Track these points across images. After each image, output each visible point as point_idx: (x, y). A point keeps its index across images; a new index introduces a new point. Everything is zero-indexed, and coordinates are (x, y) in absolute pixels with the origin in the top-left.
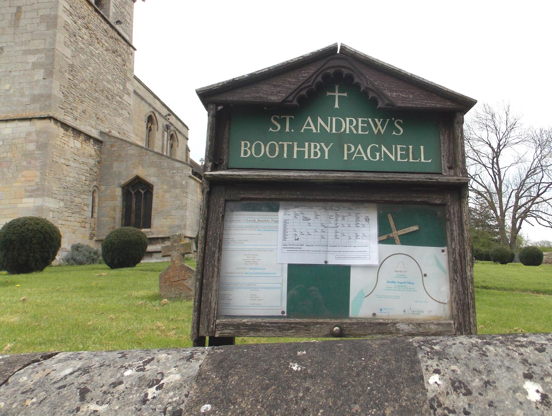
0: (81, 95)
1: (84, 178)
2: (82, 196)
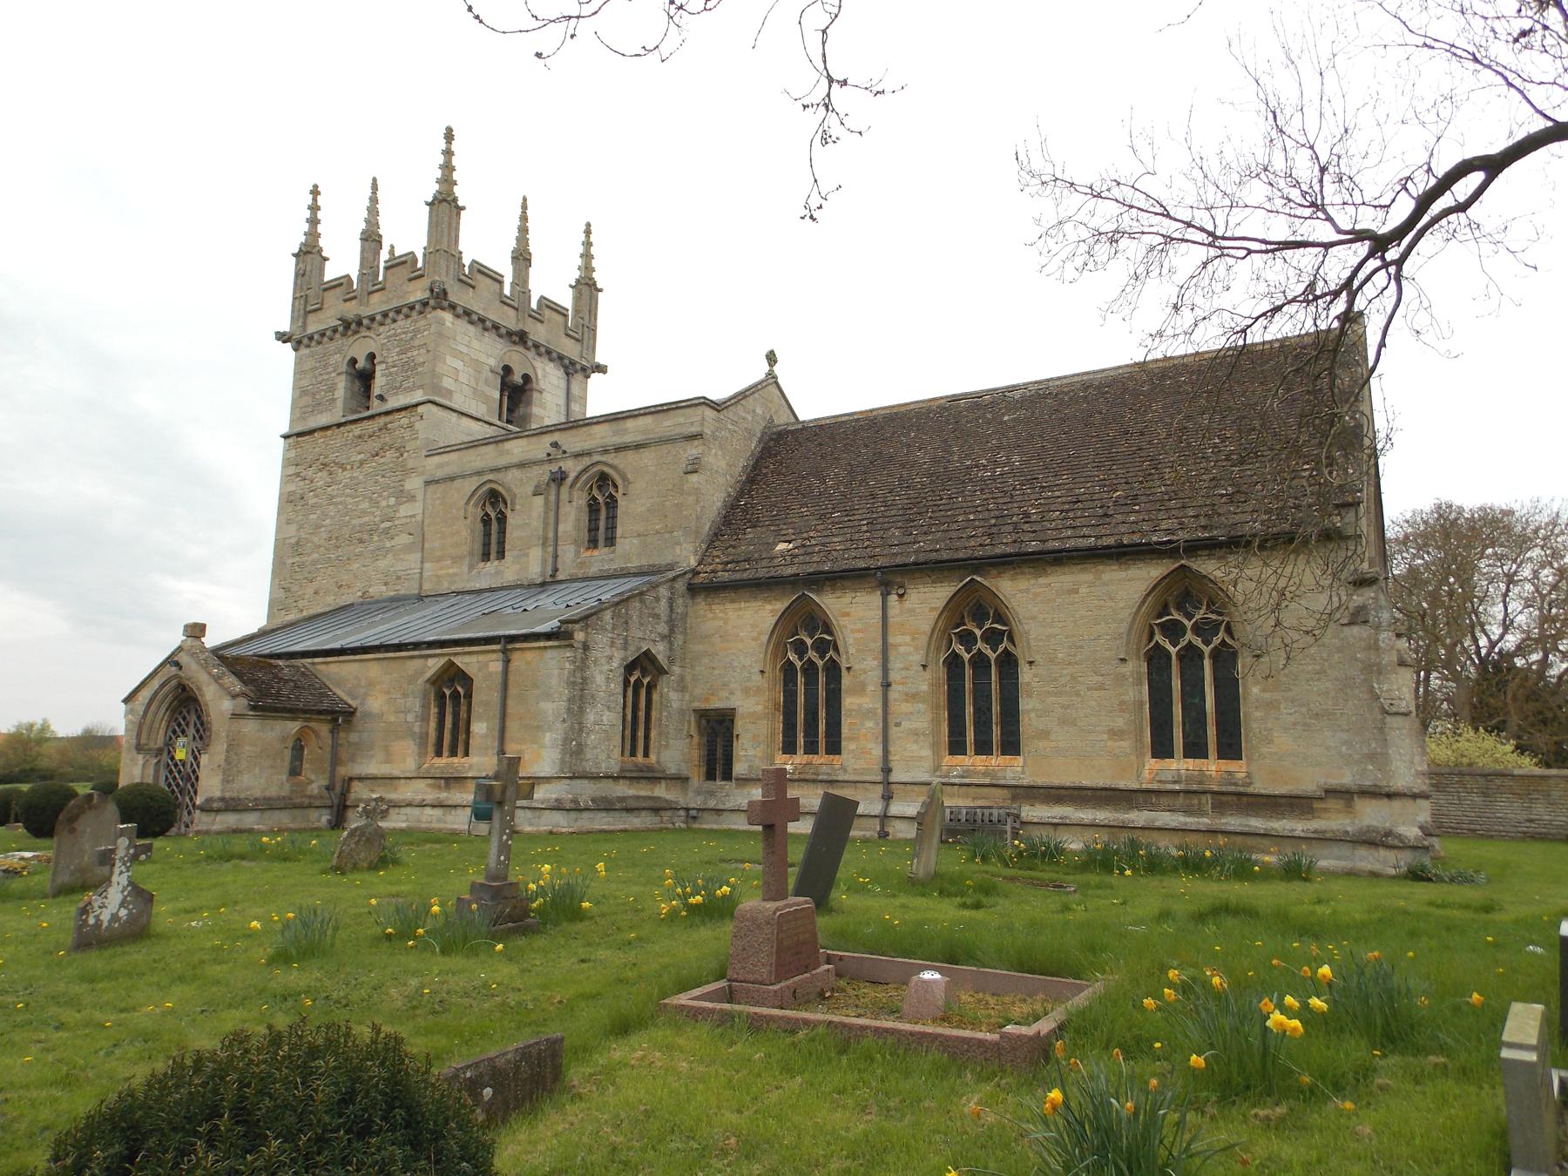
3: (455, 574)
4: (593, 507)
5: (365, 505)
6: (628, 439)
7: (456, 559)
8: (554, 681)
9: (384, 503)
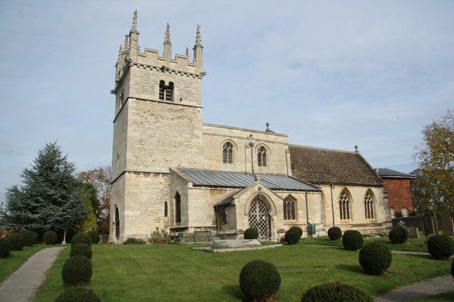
4: (259, 155)
6: (270, 140)
7: (217, 161)
9: (184, 136)
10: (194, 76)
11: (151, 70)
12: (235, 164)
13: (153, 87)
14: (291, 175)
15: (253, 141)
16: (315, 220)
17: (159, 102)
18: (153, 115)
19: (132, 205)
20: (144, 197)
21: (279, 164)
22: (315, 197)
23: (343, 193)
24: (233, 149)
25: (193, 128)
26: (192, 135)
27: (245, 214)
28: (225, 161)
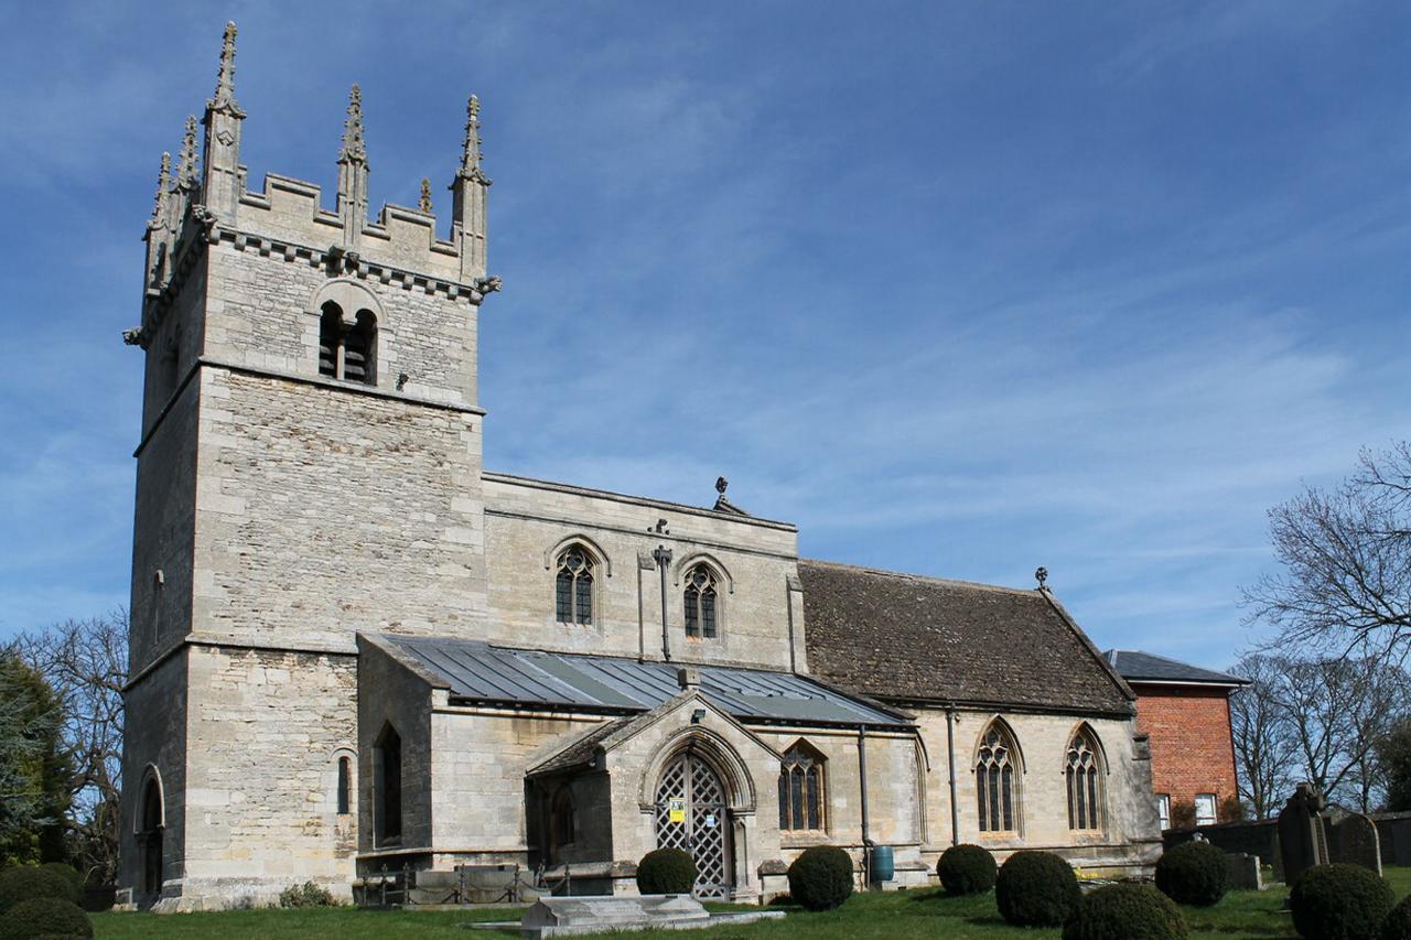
0: (283, 575)
1: (306, 738)
2: (300, 775)
3: (538, 630)
4: (690, 595)
5: (384, 510)
6: (730, 540)
7: (536, 613)
8: (901, 766)
9: (415, 516)
10: (453, 290)
11: (289, 259)
12: (600, 629)
13: (295, 327)
14: (803, 669)
15: (668, 545)
16: (892, 829)
17: (320, 386)
18: (296, 432)
19: (213, 770)
20: (262, 742)
21: (762, 625)
22: (892, 751)
23: (989, 738)
24: (594, 571)
25: (449, 488)
26: (444, 513)
27: (644, 808)
28: (563, 615)
